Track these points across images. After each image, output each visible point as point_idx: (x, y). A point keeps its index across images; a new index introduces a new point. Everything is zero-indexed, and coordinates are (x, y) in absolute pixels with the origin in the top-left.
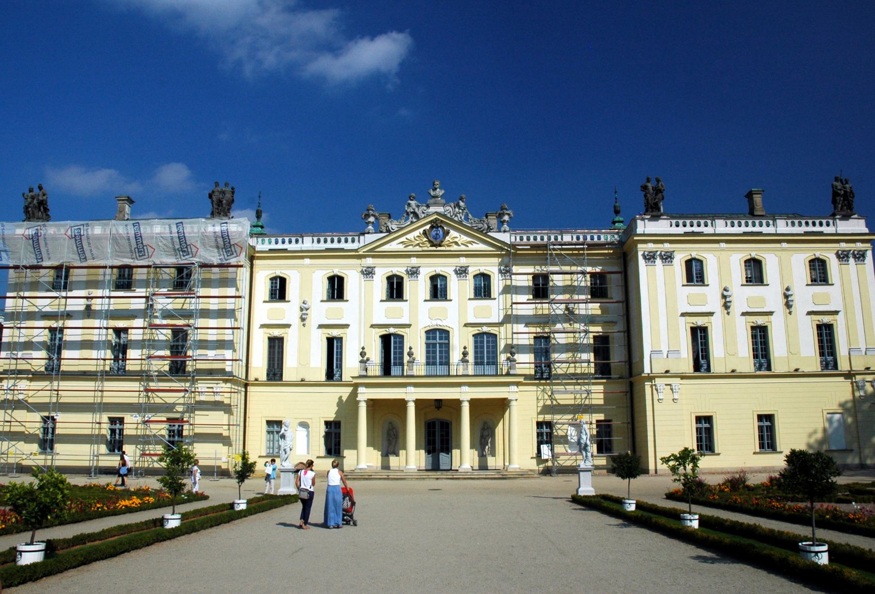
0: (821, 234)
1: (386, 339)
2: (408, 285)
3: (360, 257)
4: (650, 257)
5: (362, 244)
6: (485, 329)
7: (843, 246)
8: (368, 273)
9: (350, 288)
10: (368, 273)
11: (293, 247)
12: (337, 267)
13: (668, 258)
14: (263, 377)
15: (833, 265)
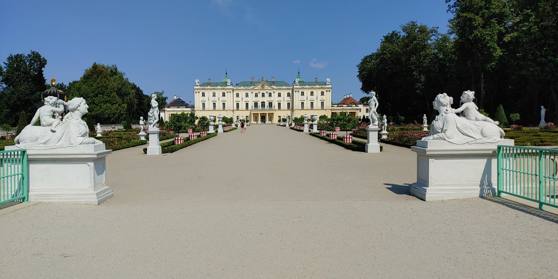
0: (323, 87)
1: (255, 103)
2: (258, 94)
3: (251, 90)
4: (296, 92)
5: (251, 88)
6: (270, 102)
7: (327, 89)
8: (252, 93)
9: (249, 96)
10: (252, 93)
11: (240, 88)
12: (247, 91)
13: (298, 92)
14: (236, 109)
15: (325, 93)
